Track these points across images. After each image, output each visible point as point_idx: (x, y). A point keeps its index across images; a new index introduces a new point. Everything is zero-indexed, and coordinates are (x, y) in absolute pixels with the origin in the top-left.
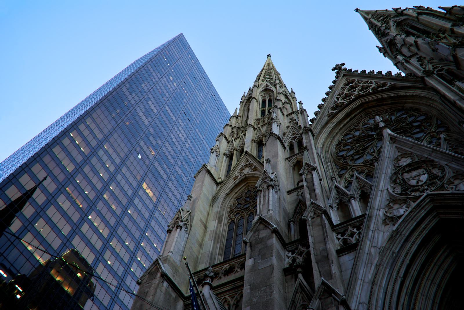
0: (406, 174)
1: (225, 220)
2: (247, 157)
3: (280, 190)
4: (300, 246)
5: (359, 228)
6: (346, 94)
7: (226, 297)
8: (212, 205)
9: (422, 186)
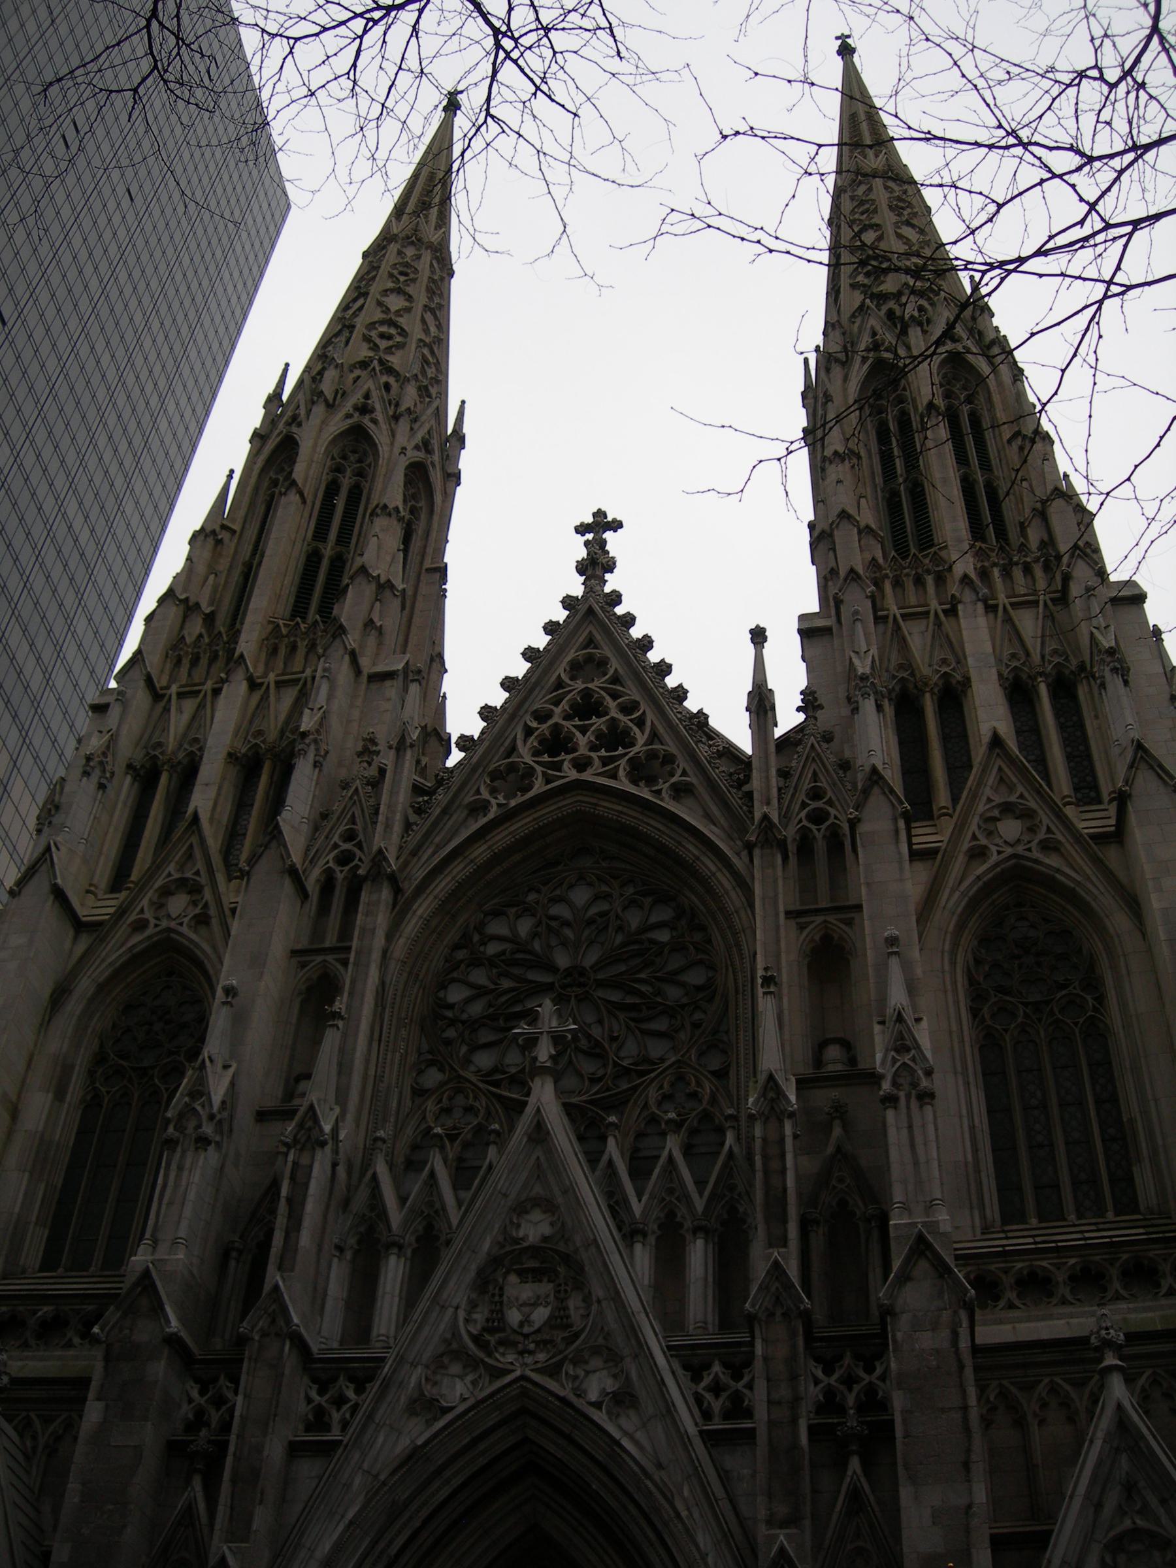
0: (513, 1278)
1: (76, 1090)
2: (194, 840)
3: (231, 1131)
4: (222, 1377)
5: (359, 1390)
6: (556, 724)
7: (33, 1415)
8: (47, 1018)
9: (526, 1336)
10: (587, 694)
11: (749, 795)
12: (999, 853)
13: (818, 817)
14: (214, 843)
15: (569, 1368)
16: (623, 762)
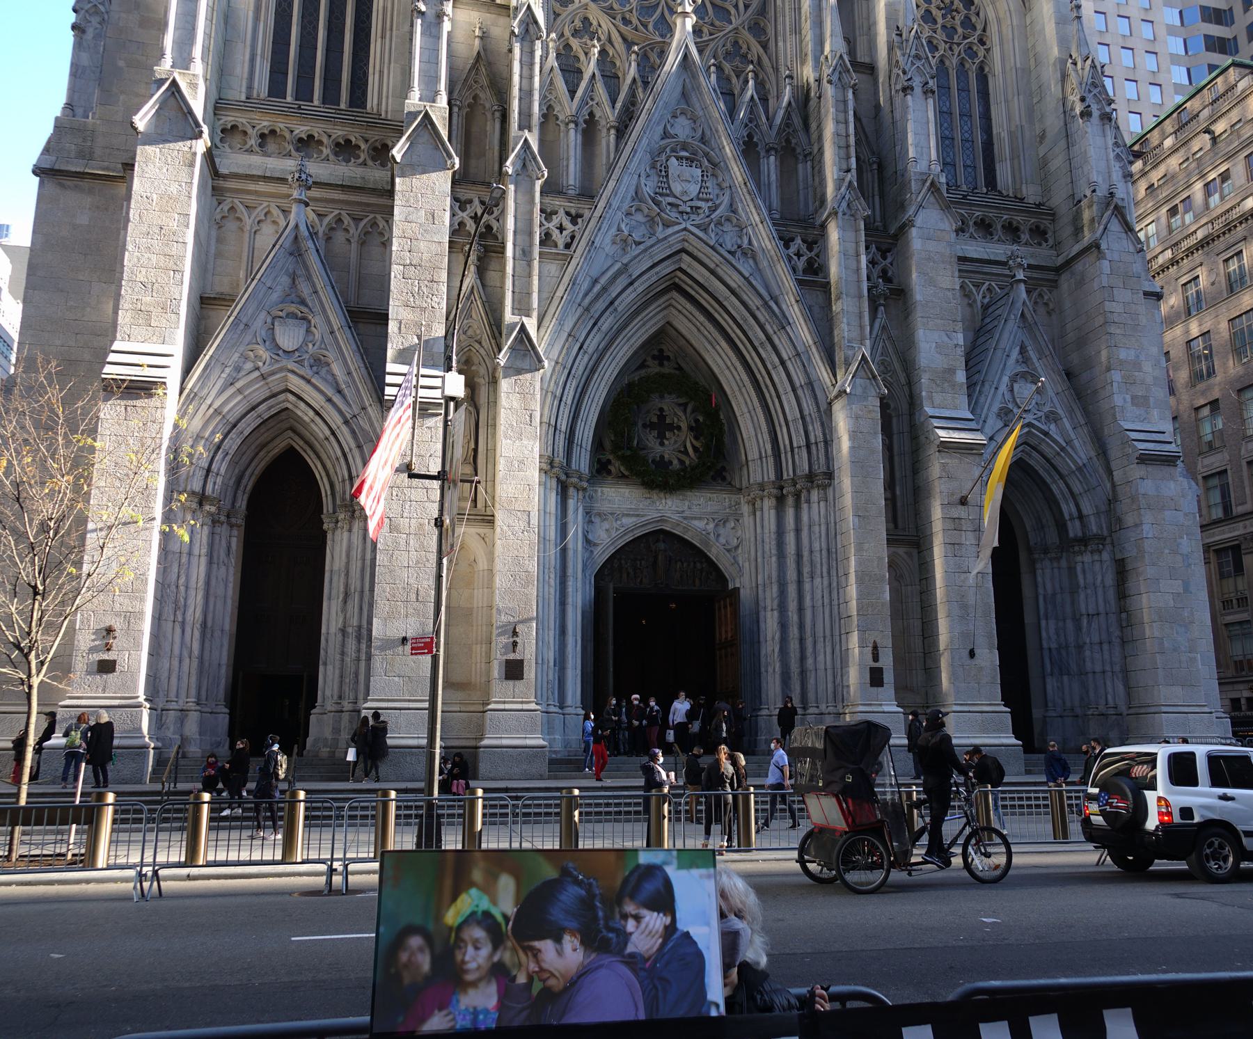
0: (673, 160)
5: (574, 222)
9: (685, 202)
15: (712, 225)
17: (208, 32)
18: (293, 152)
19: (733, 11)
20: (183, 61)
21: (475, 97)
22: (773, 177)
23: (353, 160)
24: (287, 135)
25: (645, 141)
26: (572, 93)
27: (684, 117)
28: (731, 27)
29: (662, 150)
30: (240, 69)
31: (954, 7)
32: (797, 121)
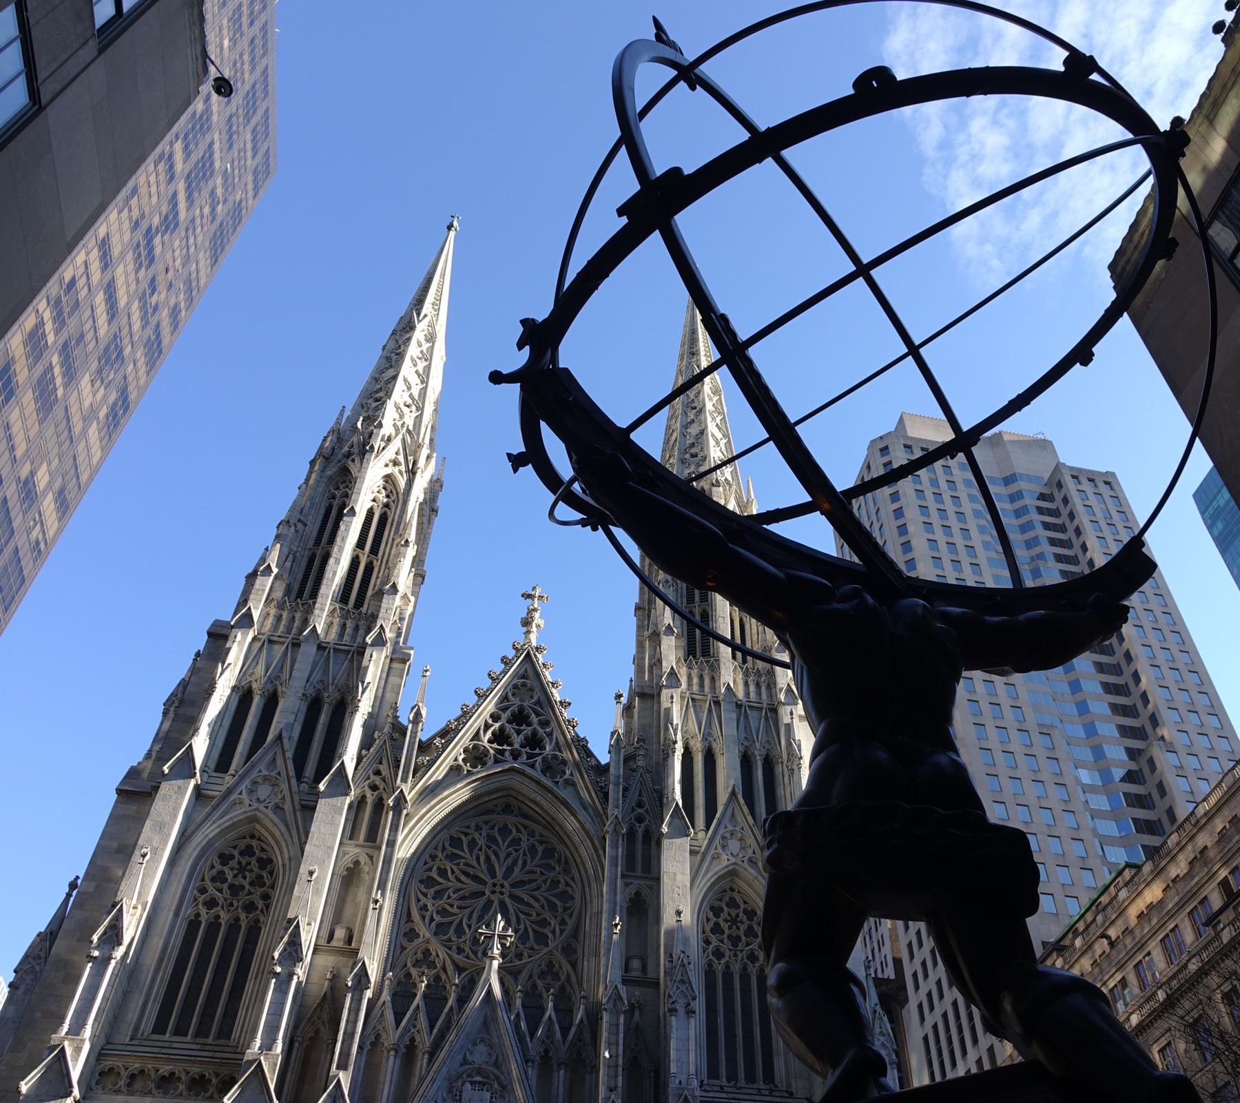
0: (468, 1085)
2: (277, 749)
10: (521, 709)
11: (606, 795)
12: (728, 860)
13: (640, 819)
14: (289, 754)
16: (539, 759)
17: (107, 995)
18: (154, 1091)
19: (550, 935)
20: (76, 1029)
21: (317, 1032)
22: (561, 1090)
23: (202, 1094)
24: (153, 1074)
25: (445, 1070)
26: (398, 1024)
27: (482, 1044)
28: (547, 950)
29: (459, 1076)
30: (132, 1016)
31: (739, 919)
32: (587, 1036)
